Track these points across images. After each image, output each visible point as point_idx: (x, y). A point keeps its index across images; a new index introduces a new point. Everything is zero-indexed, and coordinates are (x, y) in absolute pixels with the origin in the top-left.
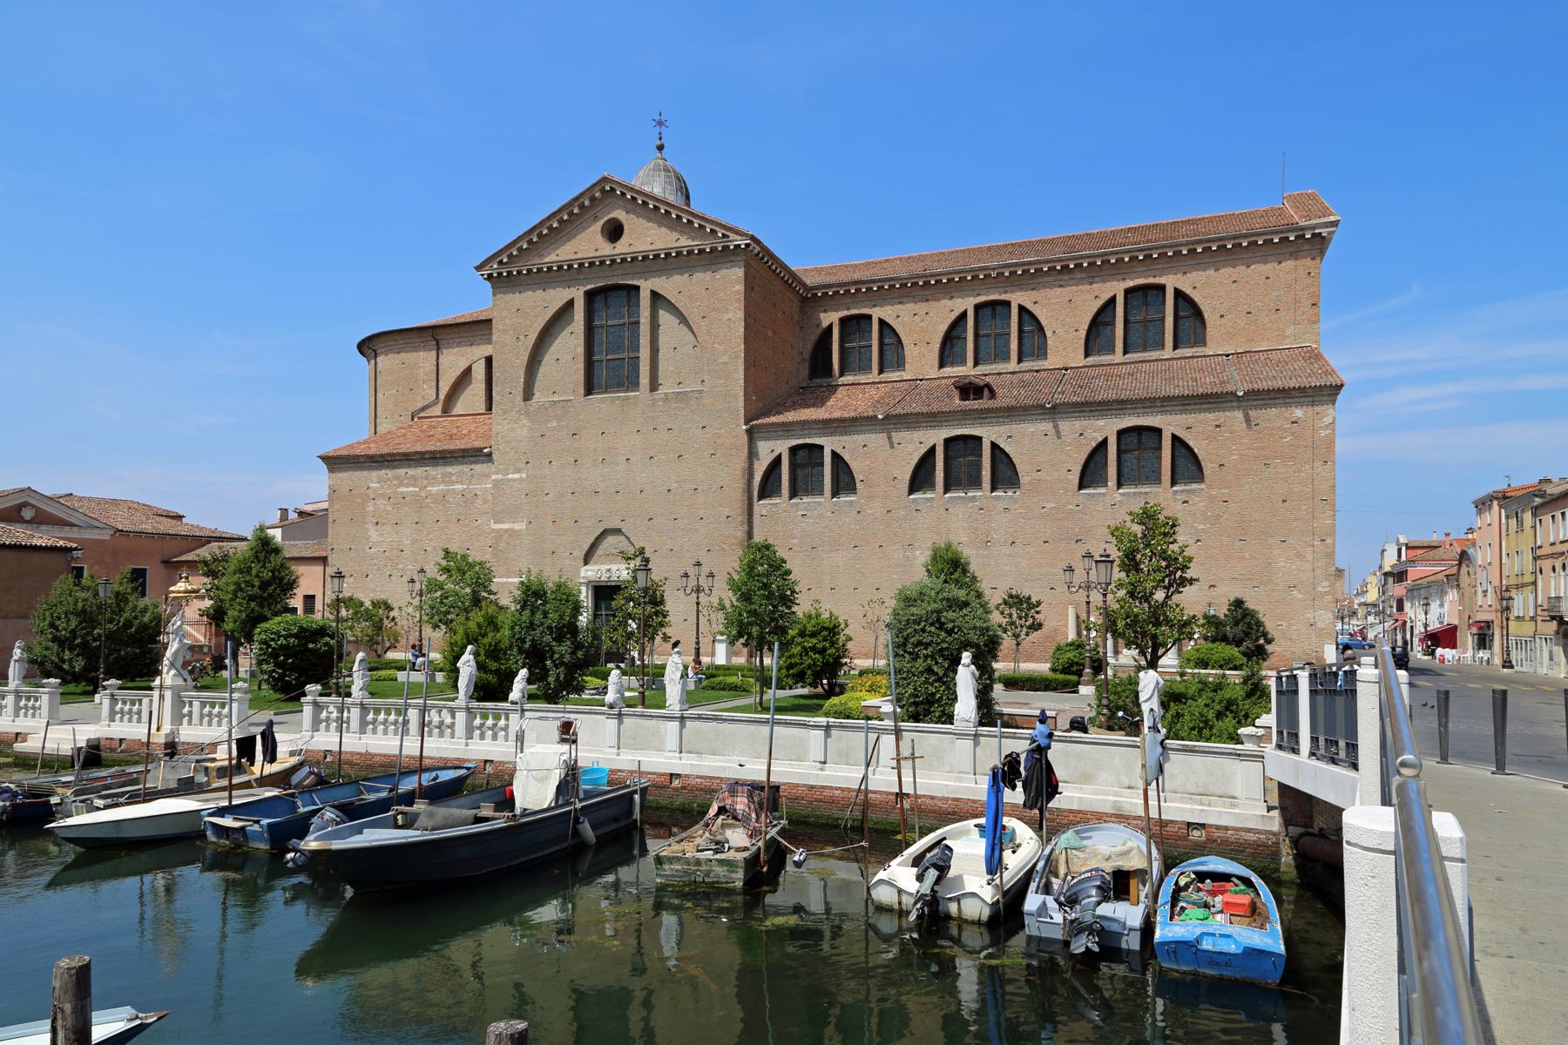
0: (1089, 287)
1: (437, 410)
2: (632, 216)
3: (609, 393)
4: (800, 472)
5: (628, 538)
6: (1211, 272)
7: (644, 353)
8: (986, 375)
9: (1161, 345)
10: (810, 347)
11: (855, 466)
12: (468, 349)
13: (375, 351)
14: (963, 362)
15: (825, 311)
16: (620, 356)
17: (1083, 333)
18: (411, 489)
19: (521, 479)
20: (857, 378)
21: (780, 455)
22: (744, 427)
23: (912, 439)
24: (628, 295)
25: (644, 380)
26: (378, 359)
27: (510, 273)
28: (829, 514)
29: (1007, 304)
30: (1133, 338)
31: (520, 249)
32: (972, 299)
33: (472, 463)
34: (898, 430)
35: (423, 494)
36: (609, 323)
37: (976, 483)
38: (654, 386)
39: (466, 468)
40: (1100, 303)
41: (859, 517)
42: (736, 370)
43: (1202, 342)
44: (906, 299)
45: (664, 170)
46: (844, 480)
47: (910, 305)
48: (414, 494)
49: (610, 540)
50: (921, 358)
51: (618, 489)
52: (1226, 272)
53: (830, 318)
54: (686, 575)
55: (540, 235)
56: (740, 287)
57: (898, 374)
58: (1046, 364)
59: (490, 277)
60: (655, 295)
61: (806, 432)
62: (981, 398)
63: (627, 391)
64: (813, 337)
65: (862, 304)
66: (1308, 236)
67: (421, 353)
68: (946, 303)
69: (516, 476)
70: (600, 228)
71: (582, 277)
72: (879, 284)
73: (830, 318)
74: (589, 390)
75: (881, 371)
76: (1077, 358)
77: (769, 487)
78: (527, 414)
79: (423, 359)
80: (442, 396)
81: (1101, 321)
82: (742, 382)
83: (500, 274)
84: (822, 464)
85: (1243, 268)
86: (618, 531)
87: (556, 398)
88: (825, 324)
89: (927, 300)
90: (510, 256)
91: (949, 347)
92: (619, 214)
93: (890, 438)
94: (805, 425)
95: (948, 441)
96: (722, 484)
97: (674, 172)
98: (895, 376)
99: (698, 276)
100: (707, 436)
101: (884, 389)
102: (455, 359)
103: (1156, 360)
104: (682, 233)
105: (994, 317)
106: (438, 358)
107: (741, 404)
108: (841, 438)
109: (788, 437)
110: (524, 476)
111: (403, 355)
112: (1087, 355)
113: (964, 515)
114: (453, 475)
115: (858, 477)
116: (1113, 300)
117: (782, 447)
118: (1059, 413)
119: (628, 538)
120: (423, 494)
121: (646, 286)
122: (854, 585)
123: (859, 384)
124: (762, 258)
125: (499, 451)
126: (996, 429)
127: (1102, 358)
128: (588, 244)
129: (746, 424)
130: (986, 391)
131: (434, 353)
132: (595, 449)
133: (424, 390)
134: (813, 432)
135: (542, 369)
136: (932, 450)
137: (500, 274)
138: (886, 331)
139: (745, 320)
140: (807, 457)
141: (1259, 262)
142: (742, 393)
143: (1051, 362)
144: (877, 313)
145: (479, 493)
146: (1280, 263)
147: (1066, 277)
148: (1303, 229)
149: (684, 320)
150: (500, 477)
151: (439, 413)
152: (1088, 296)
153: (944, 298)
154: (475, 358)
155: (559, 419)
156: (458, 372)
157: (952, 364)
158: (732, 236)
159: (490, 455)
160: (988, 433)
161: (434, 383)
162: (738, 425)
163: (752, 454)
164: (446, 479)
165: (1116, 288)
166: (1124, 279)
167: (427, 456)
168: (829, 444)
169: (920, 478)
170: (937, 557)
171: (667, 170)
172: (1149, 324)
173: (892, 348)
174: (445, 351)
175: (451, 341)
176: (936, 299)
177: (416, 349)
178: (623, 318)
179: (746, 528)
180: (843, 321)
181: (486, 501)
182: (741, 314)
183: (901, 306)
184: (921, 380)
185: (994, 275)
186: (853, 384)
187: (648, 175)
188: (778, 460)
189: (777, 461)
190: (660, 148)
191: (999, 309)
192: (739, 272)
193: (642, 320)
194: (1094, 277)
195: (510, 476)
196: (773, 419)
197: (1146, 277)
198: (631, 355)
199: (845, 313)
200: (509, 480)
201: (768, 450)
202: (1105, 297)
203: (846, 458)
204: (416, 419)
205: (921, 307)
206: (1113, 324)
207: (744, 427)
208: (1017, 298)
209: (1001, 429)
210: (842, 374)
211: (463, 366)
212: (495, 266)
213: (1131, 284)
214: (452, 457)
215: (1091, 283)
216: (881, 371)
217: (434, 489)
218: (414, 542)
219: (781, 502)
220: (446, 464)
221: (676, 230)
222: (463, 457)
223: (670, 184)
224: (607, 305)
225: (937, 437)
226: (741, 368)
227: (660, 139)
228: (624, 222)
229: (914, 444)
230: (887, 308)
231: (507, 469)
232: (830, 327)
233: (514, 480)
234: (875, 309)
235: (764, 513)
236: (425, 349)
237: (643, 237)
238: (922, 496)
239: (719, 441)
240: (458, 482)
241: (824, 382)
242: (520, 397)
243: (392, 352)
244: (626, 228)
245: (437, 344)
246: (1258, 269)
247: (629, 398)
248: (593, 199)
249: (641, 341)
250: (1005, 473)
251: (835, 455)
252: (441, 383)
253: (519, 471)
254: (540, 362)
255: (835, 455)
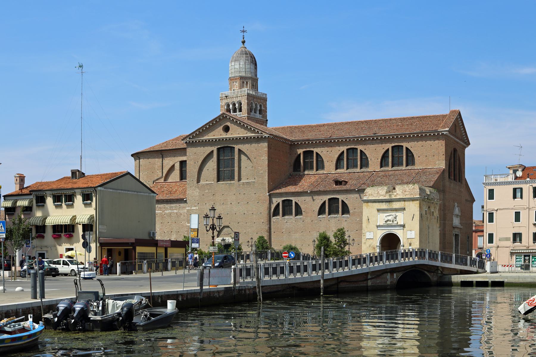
0: (381, 145)
1: (162, 180)
2: (232, 125)
3: (225, 181)
4: (286, 208)
5: (231, 229)
6: (416, 142)
7: (236, 169)
8: (350, 173)
9: (402, 165)
10: (293, 161)
11: (302, 206)
12: (173, 158)
13: (139, 158)
14: (343, 168)
15: (298, 149)
16: (229, 169)
17: (379, 160)
18: (159, 211)
19: (196, 209)
20: (309, 172)
21: (279, 203)
22: (268, 194)
23: (319, 198)
24: (231, 150)
25: (236, 178)
26: (140, 160)
27: (193, 142)
28: (294, 222)
29: (357, 149)
30: (396, 161)
31: (196, 134)
32: (346, 147)
33: (179, 203)
34: (315, 195)
35: (163, 213)
36: (225, 158)
37: (337, 212)
38: (239, 179)
39: (178, 205)
40: (384, 150)
41: (303, 223)
42: (265, 176)
43: (413, 164)
44: (324, 146)
45: (245, 54)
46: (299, 212)
47: (326, 148)
48: (161, 213)
49: (226, 229)
50: (329, 166)
51: (228, 213)
52: (420, 142)
53: (300, 151)
54: (248, 242)
55: (203, 130)
56: (266, 149)
57: (322, 171)
58: (369, 170)
59: (186, 142)
60: (239, 150)
61: (287, 196)
62: (341, 185)
63: (230, 181)
64: (294, 157)
65: (310, 147)
66: (440, 134)
67: (157, 159)
68: (338, 148)
69: (195, 208)
70: (222, 128)
71: (216, 143)
72: (315, 141)
73: (300, 151)
74: (218, 180)
75: (317, 170)
76: (378, 169)
77: (276, 213)
78: (198, 188)
79: (157, 161)
80: (164, 175)
81: (385, 156)
82: (267, 179)
83: (189, 142)
84: (292, 206)
85: (424, 142)
86: (228, 227)
87: (208, 183)
88: (299, 153)
89: (331, 147)
90: (193, 136)
91: (338, 164)
92: (228, 124)
93: (313, 198)
94: (287, 194)
95: (330, 200)
96: (261, 212)
97: (250, 54)
98: (320, 172)
99: (253, 145)
100: (256, 196)
101: (317, 177)
102: (169, 162)
103: (400, 170)
104: (248, 131)
105: (353, 153)
106: (162, 161)
107: (267, 186)
108: (298, 198)
109: (282, 197)
110: (197, 208)
111: (150, 160)
112: (381, 167)
113: (334, 222)
114: (173, 207)
115: (303, 210)
116: (388, 150)
117: (280, 200)
118: (360, 192)
119: (231, 229)
120: (163, 213)
121: (237, 147)
122: (302, 244)
123: (309, 175)
124: (274, 138)
125: (189, 199)
126: (343, 196)
127: (386, 168)
128: (218, 134)
129: (268, 193)
130: (343, 183)
131: (161, 159)
132: (220, 200)
133: (157, 173)
134: (289, 196)
135: (203, 173)
136: (325, 202)
137: (189, 142)
138: (319, 156)
139: (268, 160)
140: (287, 204)
141: (429, 140)
142: (267, 183)
143: (370, 169)
144: (315, 150)
145: (182, 213)
146: (434, 141)
147: (374, 142)
148: (439, 132)
149: (249, 158)
150: (189, 208)
151: (163, 181)
152: (381, 148)
153: (337, 146)
154: (176, 161)
155: (209, 190)
156: (170, 167)
157: (340, 168)
158: (264, 134)
159: (186, 201)
160: (341, 197)
161: (161, 170)
162: (266, 193)
163: (271, 202)
164: (171, 208)
165: (389, 146)
166: (391, 143)
167: (165, 201)
168: (294, 199)
169: (321, 211)
170: (320, 235)
171: (246, 54)
172: (400, 158)
173: (320, 165)
174: (165, 159)
175: (167, 155)
176: (334, 147)
177: (155, 158)
178: (229, 157)
179: (268, 226)
180: (304, 152)
181: (184, 216)
182: (267, 158)
183: (323, 148)
184: (330, 174)
185: (352, 140)
186: (307, 174)
187: (238, 56)
188: (278, 204)
189: (278, 204)
190: (244, 42)
191: (355, 150)
192: (266, 144)
193: (236, 158)
194: (383, 142)
195: (193, 208)
196: (277, 191)
197: (398, 143)
198: (232, 169)
199: (305, 150)
200: (192, 209)
201: (276, 201)
202: (386, 149)
203: (299, 204)
204: (154, 183)
205: (329, 149)
206: (388, 157)
207: (268, 194)
208: (360, 147)
209: (345, 196)
210: (304, 171)
211: (171, 164)
212: (188, 139)
213: (393, 145)
214: (173, 201)
215: (382, 144)
216: (317, 170)
217: (167, 212)
218: (161, 229)
219: (279, 217)
220: (171, 204)
221: (247, 130)
222: (177, 201)
223: (248, 60)
224: (224, 152)
225: (326, 198)
226: (267, 175)
227: (243, 38)
228: (230, 127)
229: (320, 200)
230: (318, 149)
231: (192, 206)
232: (300, 154)
233: (194, 209)
234: (315, 149)
235: (274, 221)
236: (158, 158)
237: (236, 132)
238: (322, 216)
239: (260, 198)
240: (175, 210)
241: (298, 173)
242: (196, 182)
243: (146, 158)
244: (230, 128)
245: (162, 156)
246: (429, 142)
247: (231, 183)
248: (220, 119)
249: (235, 165)
250: (346, 210)
251: (296, 203)
252: (164, 170)
253: (195, 206)
254: (202, 170)
255: (296, 203)
